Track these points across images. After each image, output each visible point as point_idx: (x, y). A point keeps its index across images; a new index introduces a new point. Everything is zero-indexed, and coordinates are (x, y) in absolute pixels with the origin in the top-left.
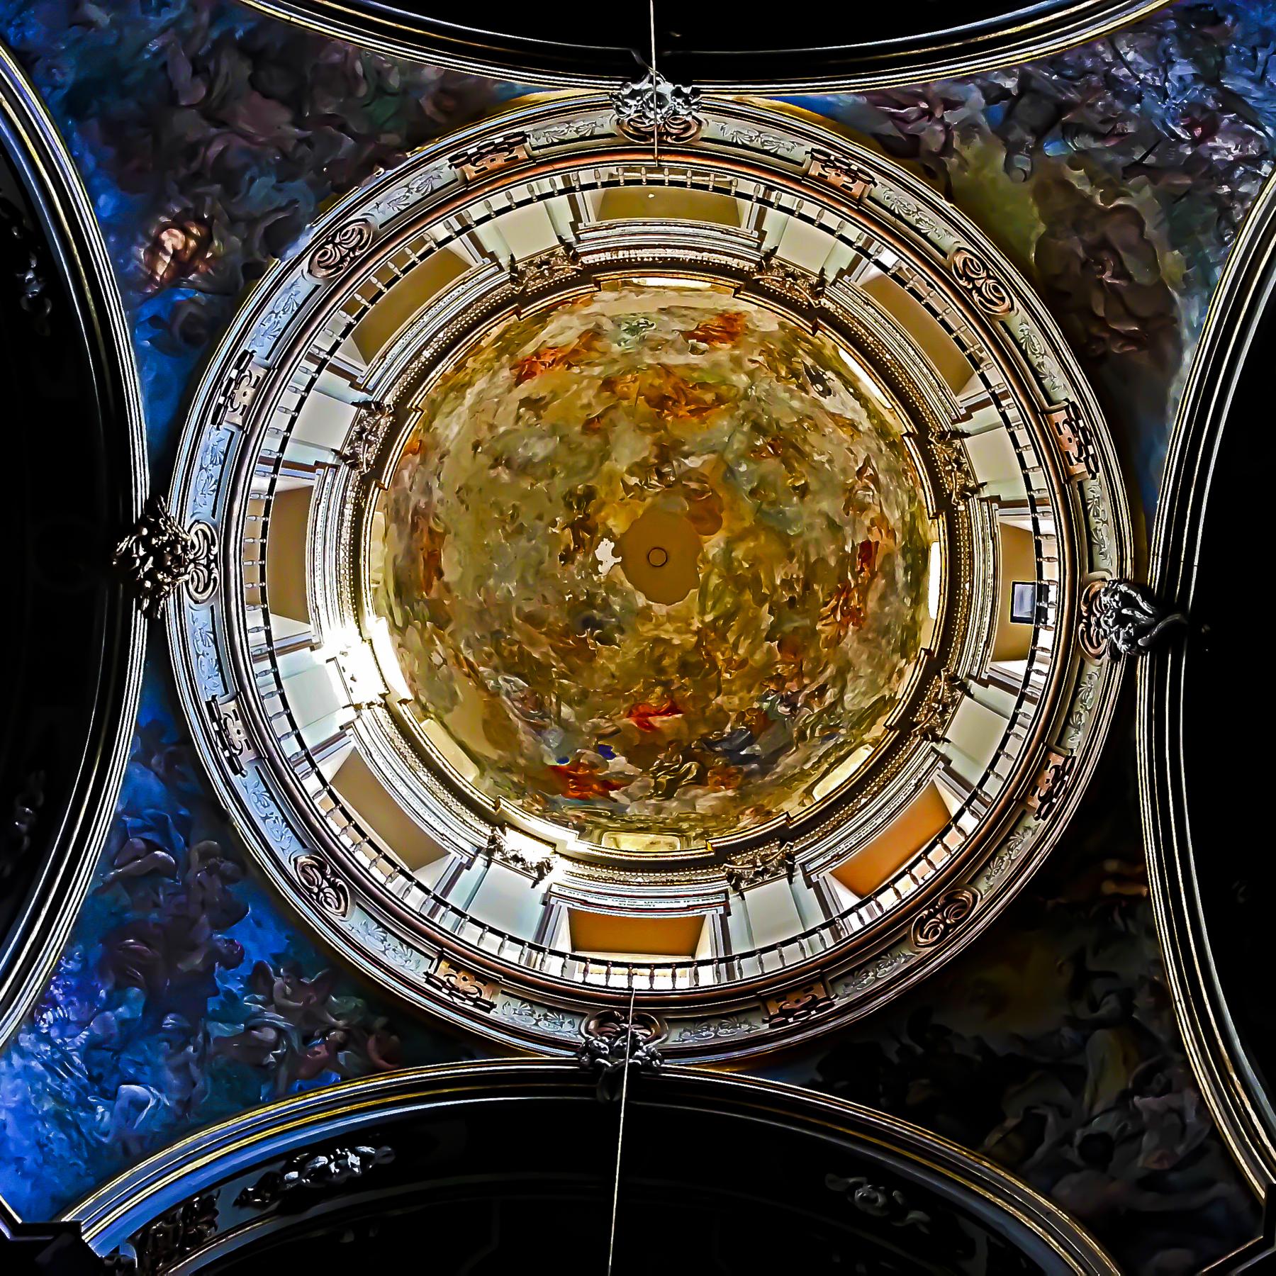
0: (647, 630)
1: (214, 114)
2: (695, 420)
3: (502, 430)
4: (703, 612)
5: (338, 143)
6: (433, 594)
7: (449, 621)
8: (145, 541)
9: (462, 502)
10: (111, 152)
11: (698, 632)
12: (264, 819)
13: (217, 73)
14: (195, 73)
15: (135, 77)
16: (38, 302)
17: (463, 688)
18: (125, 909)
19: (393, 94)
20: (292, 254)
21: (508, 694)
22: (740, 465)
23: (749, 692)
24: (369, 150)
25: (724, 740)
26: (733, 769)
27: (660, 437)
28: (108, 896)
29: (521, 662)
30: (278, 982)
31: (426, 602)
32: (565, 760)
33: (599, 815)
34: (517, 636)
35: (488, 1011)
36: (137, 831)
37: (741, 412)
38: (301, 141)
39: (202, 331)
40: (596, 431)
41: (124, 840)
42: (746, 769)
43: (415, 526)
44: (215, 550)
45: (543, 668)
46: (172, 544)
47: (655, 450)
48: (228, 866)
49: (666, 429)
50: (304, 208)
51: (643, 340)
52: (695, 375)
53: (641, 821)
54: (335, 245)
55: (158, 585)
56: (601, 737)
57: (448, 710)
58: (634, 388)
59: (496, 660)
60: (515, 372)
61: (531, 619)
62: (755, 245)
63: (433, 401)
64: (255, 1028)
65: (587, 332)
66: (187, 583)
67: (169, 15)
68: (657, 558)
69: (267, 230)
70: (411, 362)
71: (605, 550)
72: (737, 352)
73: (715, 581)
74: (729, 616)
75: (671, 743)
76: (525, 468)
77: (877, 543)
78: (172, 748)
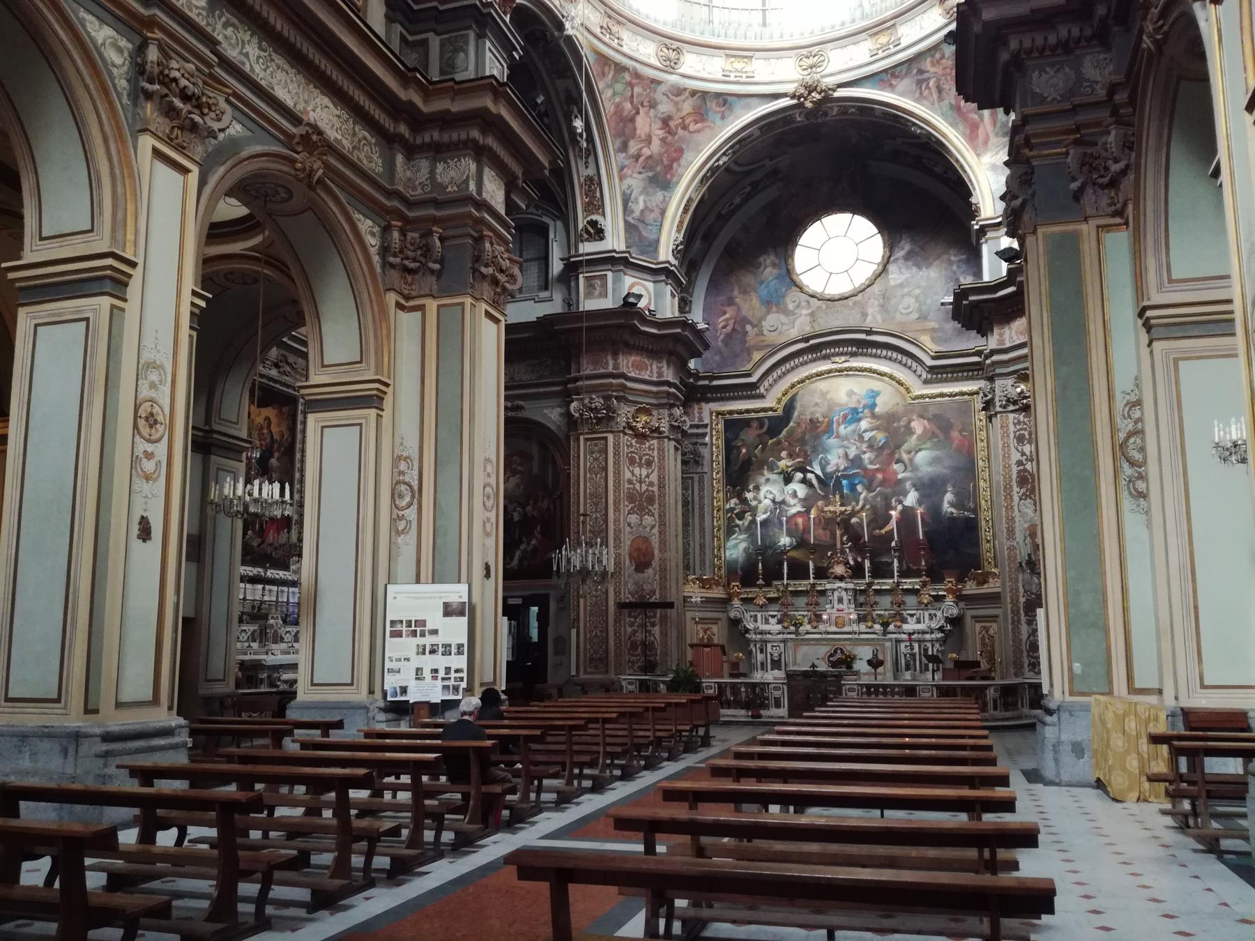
5: (639, 95)
8: (806, 99)
10: (675, 165)
24: (634, 81)
36: (921, 93)
39: (721, 100)
41: (925, 98)
48: (938, 56)
55: (822, 91)
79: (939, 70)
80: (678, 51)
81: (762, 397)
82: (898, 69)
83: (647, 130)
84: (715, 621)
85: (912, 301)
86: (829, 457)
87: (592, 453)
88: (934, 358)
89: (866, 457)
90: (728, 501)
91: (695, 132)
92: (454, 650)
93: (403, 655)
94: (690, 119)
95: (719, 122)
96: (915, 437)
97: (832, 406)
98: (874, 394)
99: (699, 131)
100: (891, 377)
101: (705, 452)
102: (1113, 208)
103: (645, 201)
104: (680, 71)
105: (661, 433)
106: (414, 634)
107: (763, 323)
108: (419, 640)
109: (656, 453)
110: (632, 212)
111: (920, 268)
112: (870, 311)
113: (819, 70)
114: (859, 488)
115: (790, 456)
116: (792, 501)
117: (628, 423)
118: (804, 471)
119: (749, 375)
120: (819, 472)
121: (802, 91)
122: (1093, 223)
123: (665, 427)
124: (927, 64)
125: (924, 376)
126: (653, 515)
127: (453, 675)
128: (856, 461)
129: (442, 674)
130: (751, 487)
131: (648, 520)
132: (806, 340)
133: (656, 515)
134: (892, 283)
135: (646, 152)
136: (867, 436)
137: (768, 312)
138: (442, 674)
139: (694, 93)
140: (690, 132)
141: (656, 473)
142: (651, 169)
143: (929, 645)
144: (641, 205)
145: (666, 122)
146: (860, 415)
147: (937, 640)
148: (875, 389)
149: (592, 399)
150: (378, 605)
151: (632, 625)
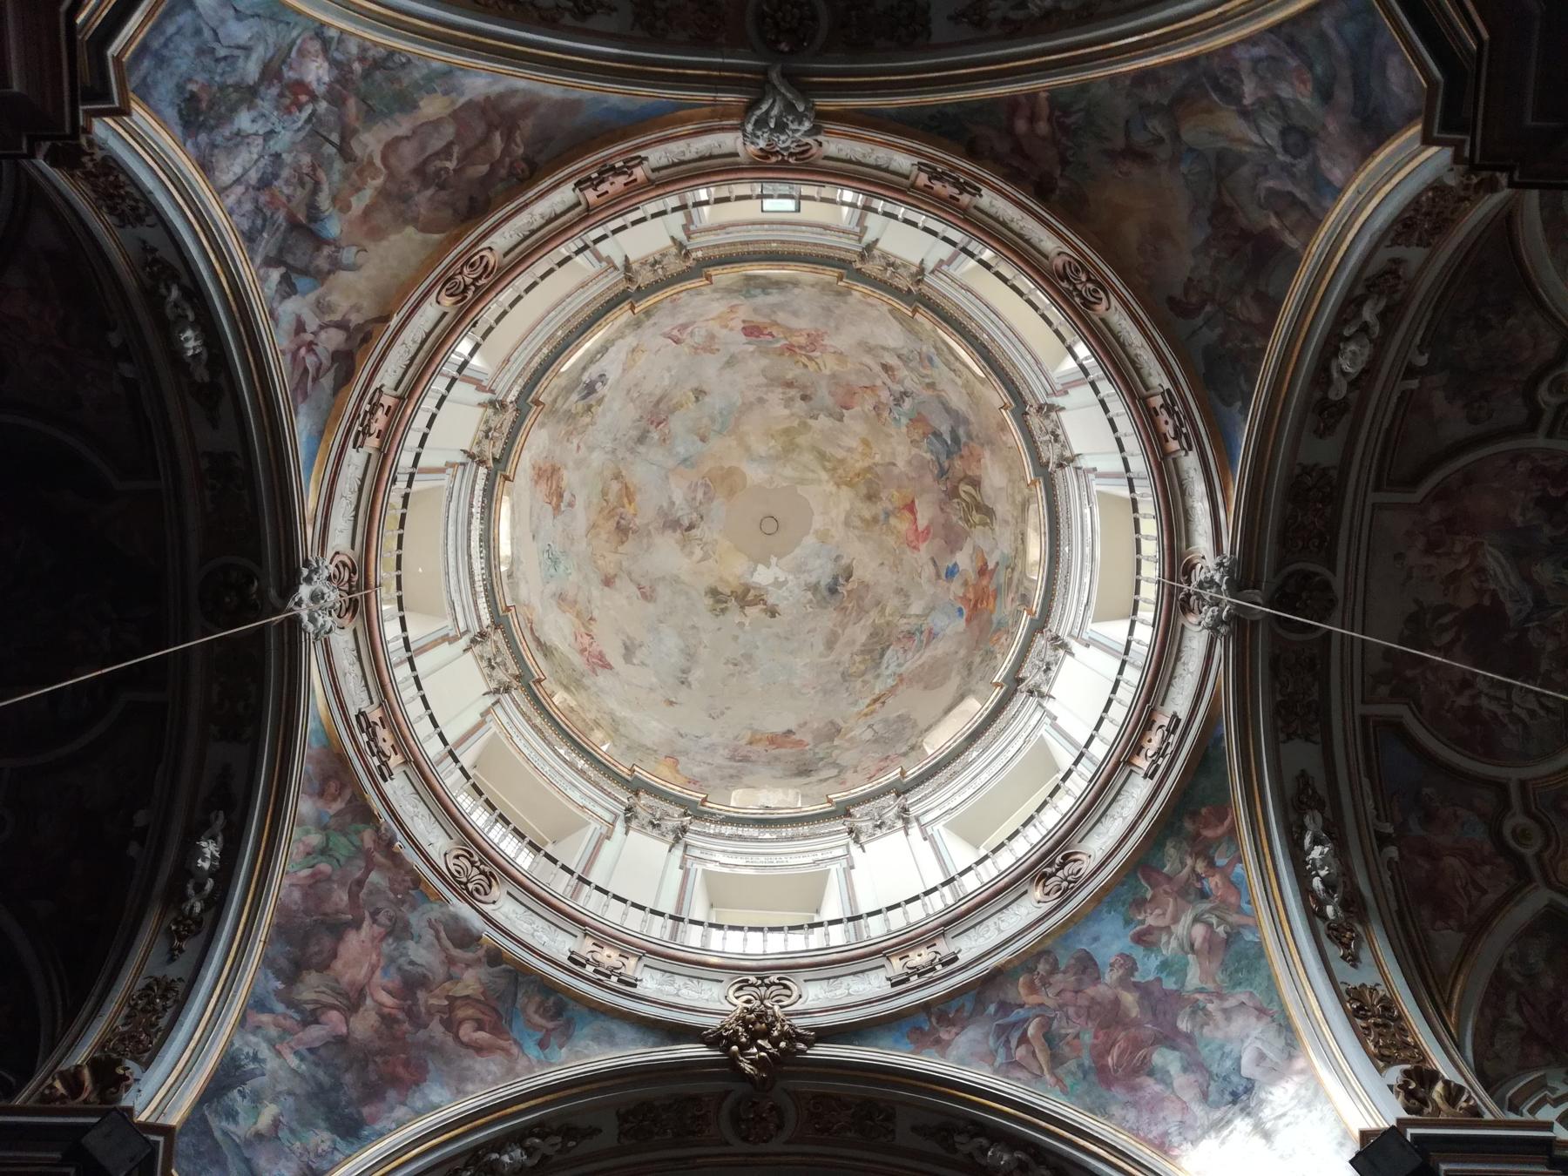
0: (838, 533)
1: (352, 1001)
2: (638, 498)
3: (654, 680)
4: (820, 481)
6: (808, 738)
7: (832, 723)
9: (722, 713)
10: (392, 1095)
11: (838, 485)
12: (1000, 931)
13: (316, 1002)
14: (317, 1022)
15: (321, 1075)
16: (529, 1151)
17: (894, 708)
18: (1080, 1066)
19: (328, 839)
20: (477, 923)
21: (900, 665)
22: (678, 453)
23: (892, 436)
24: (379, 857)
25: (938, 459)
26: (965, 452)
27: (656, 529)
28: (1068, 1081)
29: (871, 651)
30: (1151, 921)
31: (816, 746)
32: (960, 610)
33: (1011, 579)
34: (847, 657)
35: (1179, 721)
37: (628, 455)
38: (375, 921)
39: (552, 1000)
40: (653, 590)
41: (1018, 1065)
42: (963, 439)
43: (745, 759)
44: (752, 979)
45: (875, 634)
46: (745, 1022)
47: (669, 532)
48: (1042, 967)
49: (648, 524)
50: (435, 912)
51: (564, 552)
52: (595, 501)
53: (1016, 540)
54: (468, 881)
55: (784, 1035)
56: (938, 576)
57: (915, 725)
58: (611, 557)
59: (868, 677)
60: (599, 670)
61: (830, 644)
62: (461, 468)
63: (629, 748)
64: (1192, 946)
65: (559, 606)
66: (781, 1007)
67: (265, 1051)
68: (770, 526)
69: (456, 946)
70: (589, 780)
71: (763, 576)
72: (571, 464)
73: (788, 471)
74: (822, 456)
75: (942, 509)
76: (690, 655)
77: (744, 321)
78: (934, 1020)
79: (1048, 998)
80: (490, 876)
82: (955, 1004)
83: (361, 974)
91: (467, 1046)
94: (470, 1012)
95: (533, 1052)
99: (479, 1049)
104: (487, 908)
124: (1020, 991)
139: (495, 957)
140: (457, 1037)
145: (412, 984)
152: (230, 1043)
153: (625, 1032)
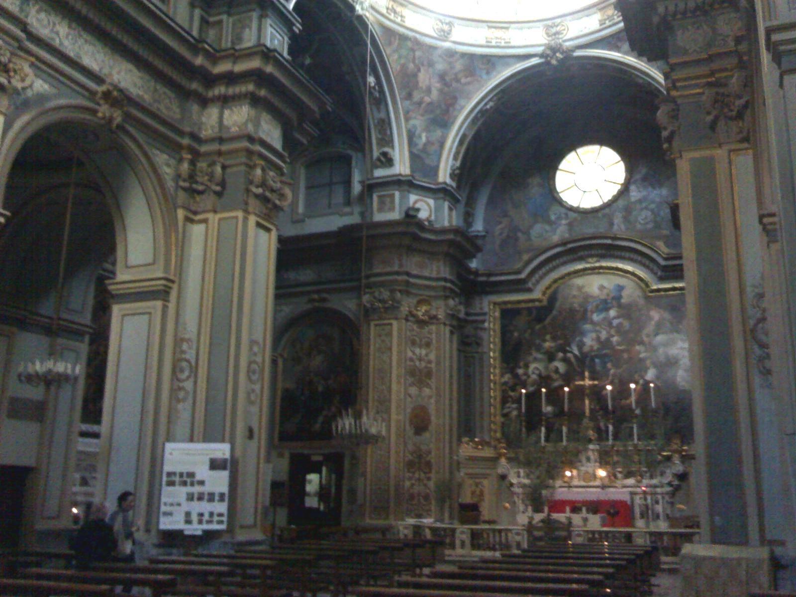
8: (552, 58)
10: (451, 109)
81: (530, 290)
83: (427, 82)
84: (485, 476)
85: (649, 213)
86: (585, 340)
87: (380, 336)
88: (666, 259)
89: (615, 339)
90: (502, 375)
92: (217, 498)
93: (176, 500)
95: (485, 77)
96: (653, 323)
97: (587, 297)
98: (621, 288)
99: (469, 83)
100: (633, 274)
101: (484, 335)
102: (741, 135)
103: (427, 138)
105: (438, 319)
106: (184, 484)
107: (531, 231)
108: (189, 489)
109: (434, 336)
110: (416, 145)
111: (654, 188)
112: (616, 221)
113: (560, 36)
114: (609, 365)
115: (554, 339)
116: (555, 376)
117: (410, 312)
118: (565, 352)
119: (519, 272)
120: (576, 352)
121: (549, 52)
122: (726, 148)
123: (441, 315)
125: (659, 273)
126: (431, 388)
127: (216, 518)
128: (605, 344)
129: (206, 517)
130: (522, 364)
131: (427, 391)
132: (564, 244)
133: (433, 386)
134: (633, 199)
135: (427, 99)
136: (615, 322)
137: (536, 222)
138: (206, 517)
139: (463, 55)
141: (434, 352)
142: (432, 111)
143: (660, 497)
144: (424, 139)
145: (442, 77)
146: (610, 305)
147: (667, 493)
148: (621, 284)
149: (380, 292)
150: (156, 461)
151: (410, 479)
152: (406, 128)
153: (511, 61)
